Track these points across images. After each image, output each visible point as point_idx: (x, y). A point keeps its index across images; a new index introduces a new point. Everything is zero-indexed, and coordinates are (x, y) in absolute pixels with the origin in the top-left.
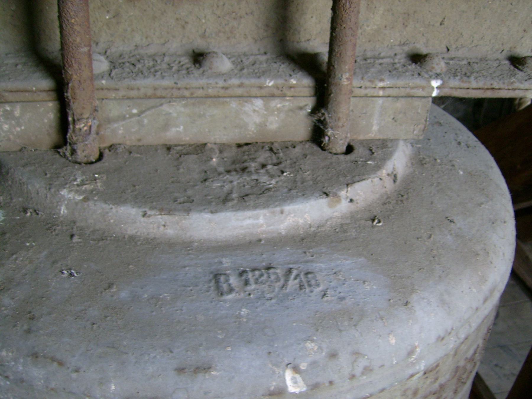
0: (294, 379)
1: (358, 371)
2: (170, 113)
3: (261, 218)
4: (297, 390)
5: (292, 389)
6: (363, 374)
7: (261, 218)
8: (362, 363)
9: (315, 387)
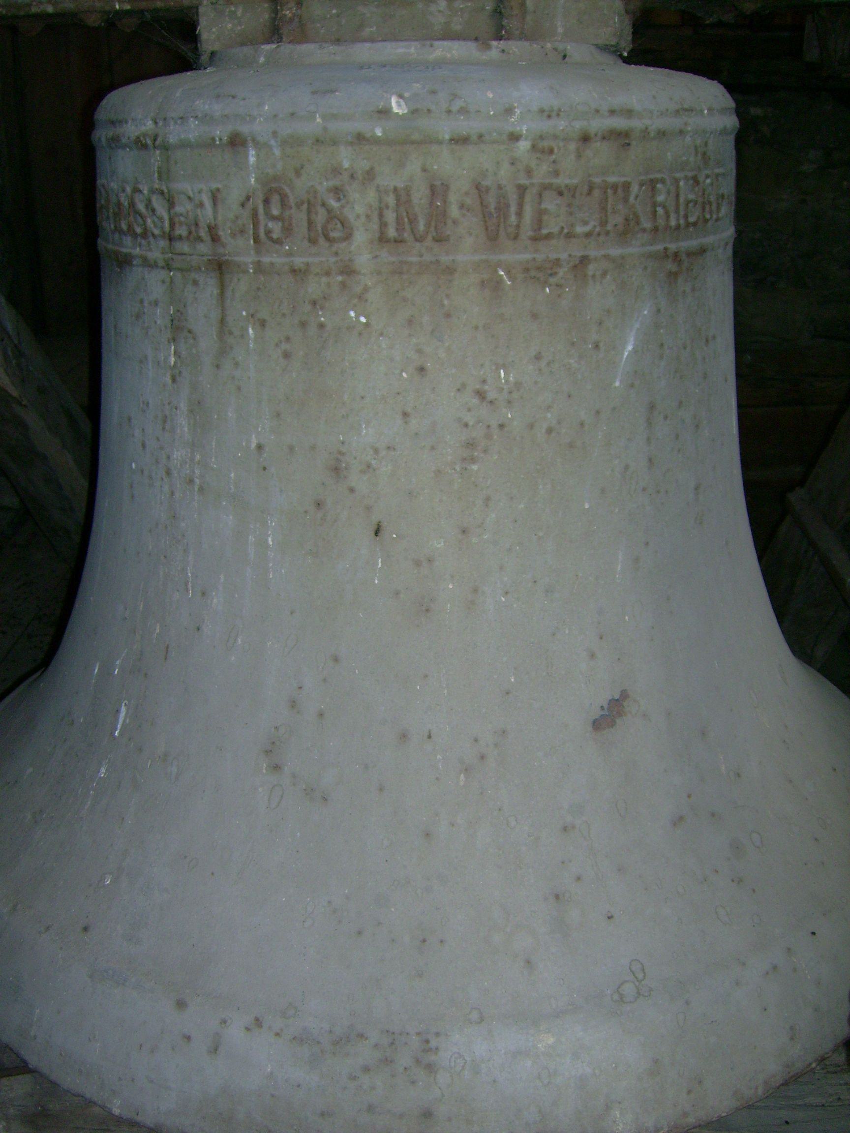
0: (398, 103)
1: (454, 109)
2: (365, 14)
3: (413, 48)
4: (400, 112)
5: (395, 109)
6: (459, 112)
7: (413, 48)
8: (458, 104)
9: (414, 112)
